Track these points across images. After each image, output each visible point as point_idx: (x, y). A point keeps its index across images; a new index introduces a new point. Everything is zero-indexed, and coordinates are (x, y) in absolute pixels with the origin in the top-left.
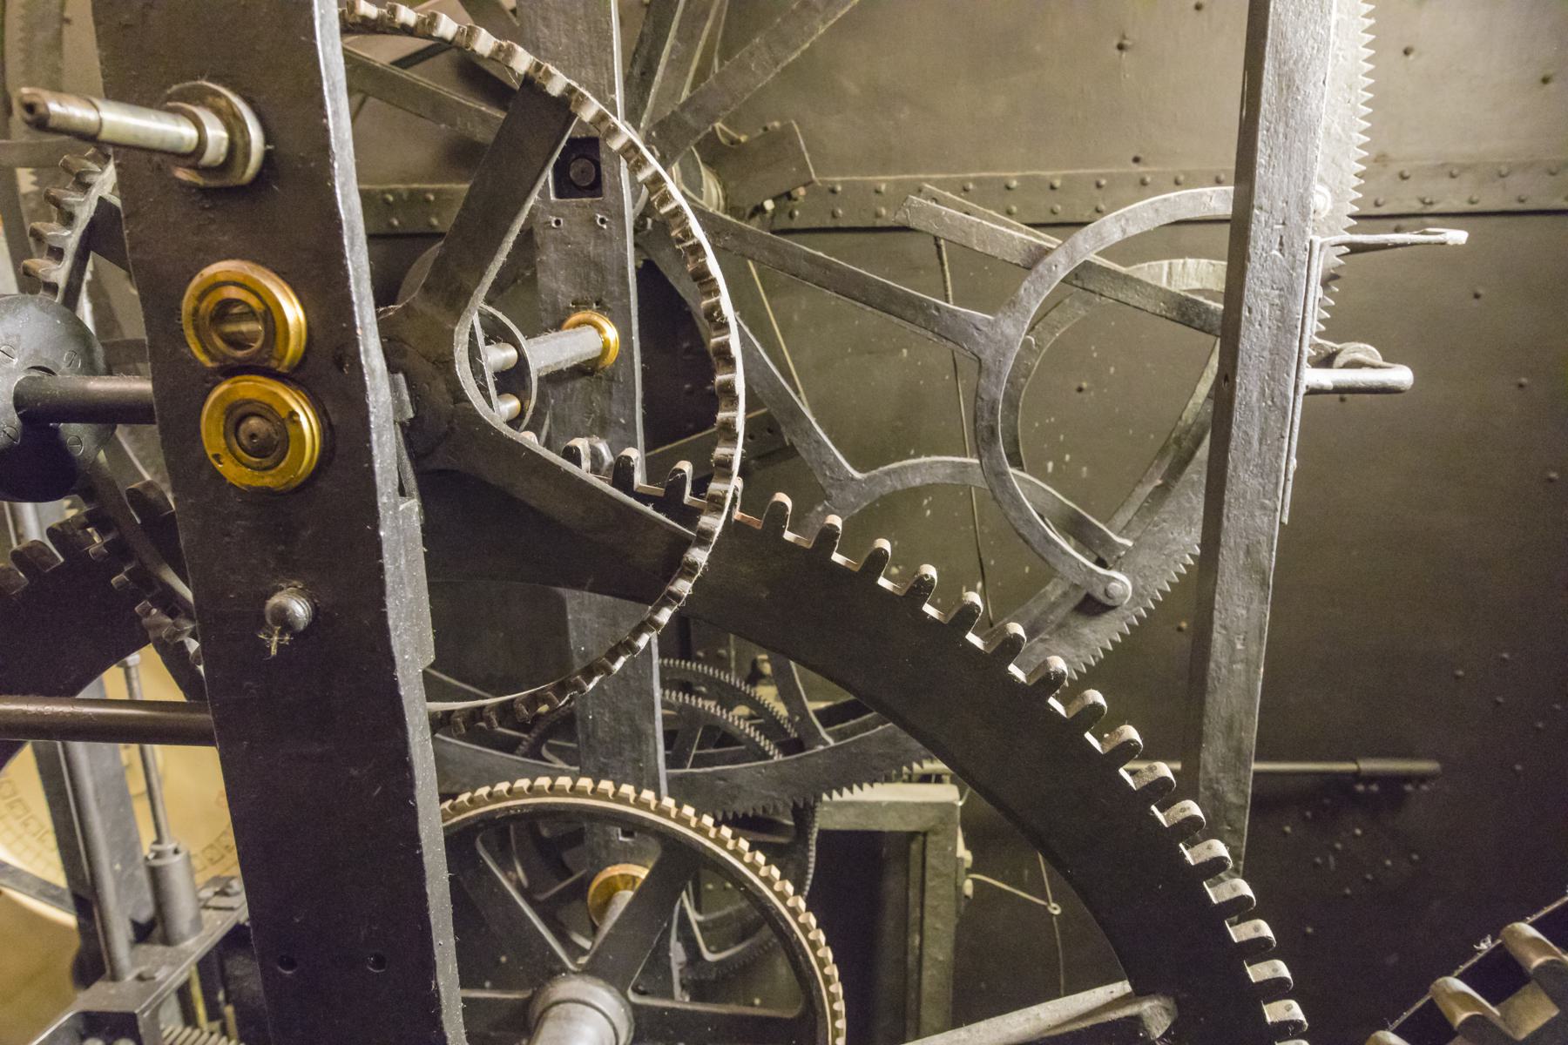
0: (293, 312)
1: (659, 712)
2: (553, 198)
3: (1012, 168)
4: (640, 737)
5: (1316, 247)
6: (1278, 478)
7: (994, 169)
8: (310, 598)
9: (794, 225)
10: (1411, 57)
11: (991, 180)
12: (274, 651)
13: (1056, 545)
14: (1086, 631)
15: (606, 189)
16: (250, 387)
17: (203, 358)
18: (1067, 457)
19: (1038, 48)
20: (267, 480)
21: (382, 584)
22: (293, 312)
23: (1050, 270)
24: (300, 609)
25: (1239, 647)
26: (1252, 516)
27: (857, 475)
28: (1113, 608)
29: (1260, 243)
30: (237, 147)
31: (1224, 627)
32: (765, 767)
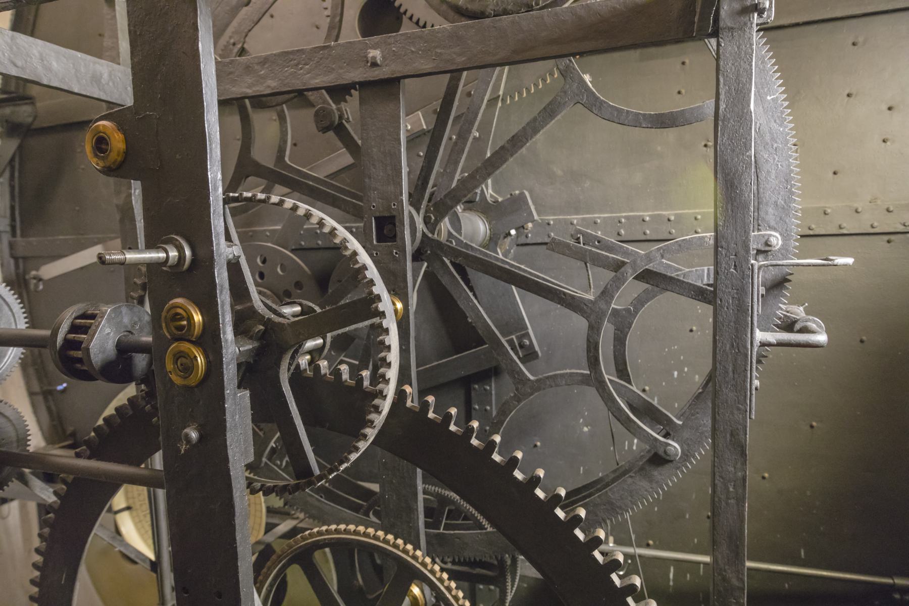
0: (198, 318)
1: (421, 497)
2: (375, 242)
3: (646, 210)
4: (411, 510)
5: (756, 268)
6: (746, 393)
7: (637, 211)
8: (199, 432)
9: (528, 241)
10: (888, 143)
11: (634, 217)
12: (183, 452)
13: (635, 422)
14: (656, 473)
15: (398, 239)
16: (185, 346)
17: (167, 334)
18: (686, 369)
19: (659, 148)
20: (185, 382)
21: (225, 426)
22: (198, 318)
23: (623, 276)
24: (194, 435)
25: (731, 489)
26: (732, 413)
27: (532, 378)
28: (671, 461)
29: (723, 265)
30: (181, 257)
31: (721, 477)
32: (481, 534)
